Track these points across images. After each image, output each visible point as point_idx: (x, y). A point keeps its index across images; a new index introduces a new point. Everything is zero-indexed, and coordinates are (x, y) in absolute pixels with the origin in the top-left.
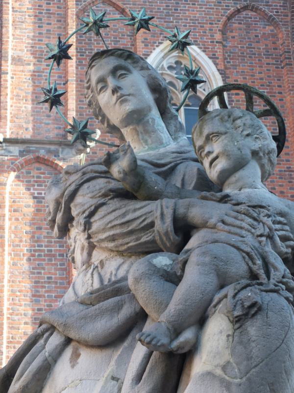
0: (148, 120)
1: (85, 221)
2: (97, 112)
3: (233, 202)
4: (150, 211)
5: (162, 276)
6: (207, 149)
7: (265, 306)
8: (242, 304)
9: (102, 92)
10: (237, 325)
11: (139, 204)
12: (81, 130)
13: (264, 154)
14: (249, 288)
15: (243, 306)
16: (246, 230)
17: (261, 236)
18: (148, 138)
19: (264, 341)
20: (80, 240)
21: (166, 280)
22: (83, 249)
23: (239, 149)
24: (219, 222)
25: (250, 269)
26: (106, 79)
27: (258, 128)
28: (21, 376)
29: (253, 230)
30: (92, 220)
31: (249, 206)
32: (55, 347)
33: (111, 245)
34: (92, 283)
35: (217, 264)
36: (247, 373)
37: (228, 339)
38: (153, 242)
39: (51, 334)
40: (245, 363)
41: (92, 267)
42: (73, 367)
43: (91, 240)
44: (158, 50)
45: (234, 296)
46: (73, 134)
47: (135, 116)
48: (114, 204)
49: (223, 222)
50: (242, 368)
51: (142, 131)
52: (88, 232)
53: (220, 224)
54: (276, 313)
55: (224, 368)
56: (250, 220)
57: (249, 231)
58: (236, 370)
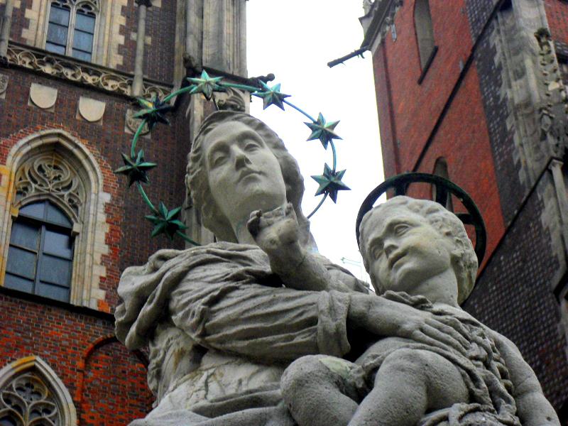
1: (203, 309)
2: (203, 195)
5: (336, 383)
13: (465, 265)
14: (478, 413)
24: (417, 329)
31: (457, 318)
43: (207, 338)
44: (9, 367)
45: (461, 419)
48: (253, 289)
49: (422, 330)
53: (418, 332)
56: (460, 335)
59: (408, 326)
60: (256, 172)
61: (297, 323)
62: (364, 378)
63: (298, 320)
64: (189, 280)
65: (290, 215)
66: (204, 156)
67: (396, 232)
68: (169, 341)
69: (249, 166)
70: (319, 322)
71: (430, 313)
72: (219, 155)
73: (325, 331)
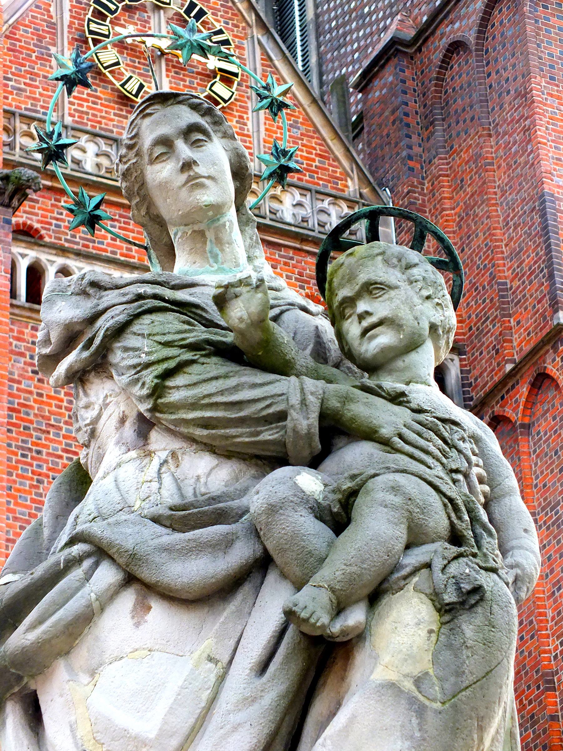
0: (225, 222)
1: (157, 384)
2: (136, 189)
3: (413, 405)
4: (280, 392)
5: (311, 508)
6: (362, 306)
7: (488, 595)
8: (457, 583)
9: (157, 161)
10: (447, 618)
11: (261, 377)
12: (91, 211)
13: (443, 332)
14: (461, 560)
15: (459, 589)
16: (434, 458)
17: (457, 471)
18: (219, 252)
19: (484, 650)
20: (117, 403)
21: (316, 517)
22: (122, 421)
23: (416, 319)
25: (452, 524)
26: (173, 142)
27: (440, 288)
28: (40, 621)
29: (444, 460)
30: (170, 383)
32: (107, 586)
33: (199, 432)
34: (160, 488)
35: (411, 510)
36: (454, 697)
37: (430, 636)
38: (282, 444)
39: (96, 565)
40: (452, 679)
41: (156, 462)
42: (137, 625)
43: (158, 415)
46: (75, 215)
47: (210, 213)
49: (401, 436)
50: (447, 686)
51: (213, 239)
52: (156, 400)
53: (396, 439)
54: (502, 609)
55: (418, 682)
56: (440, 442)
57: (438, 460)
58: (437, 688)
59: (386, 431)
60: (204, 177)
61: (264, 416)
62: (340, 501)
63: (264, 413)
64: (135, 334)
65: (260, 289)
66: (143, 145)
67: (370, 293)
68: (106, 396)
69: (196, 169)
70: (289, 418)
71: (409, 411)
72: (159, 150)
73: (294, 430)
